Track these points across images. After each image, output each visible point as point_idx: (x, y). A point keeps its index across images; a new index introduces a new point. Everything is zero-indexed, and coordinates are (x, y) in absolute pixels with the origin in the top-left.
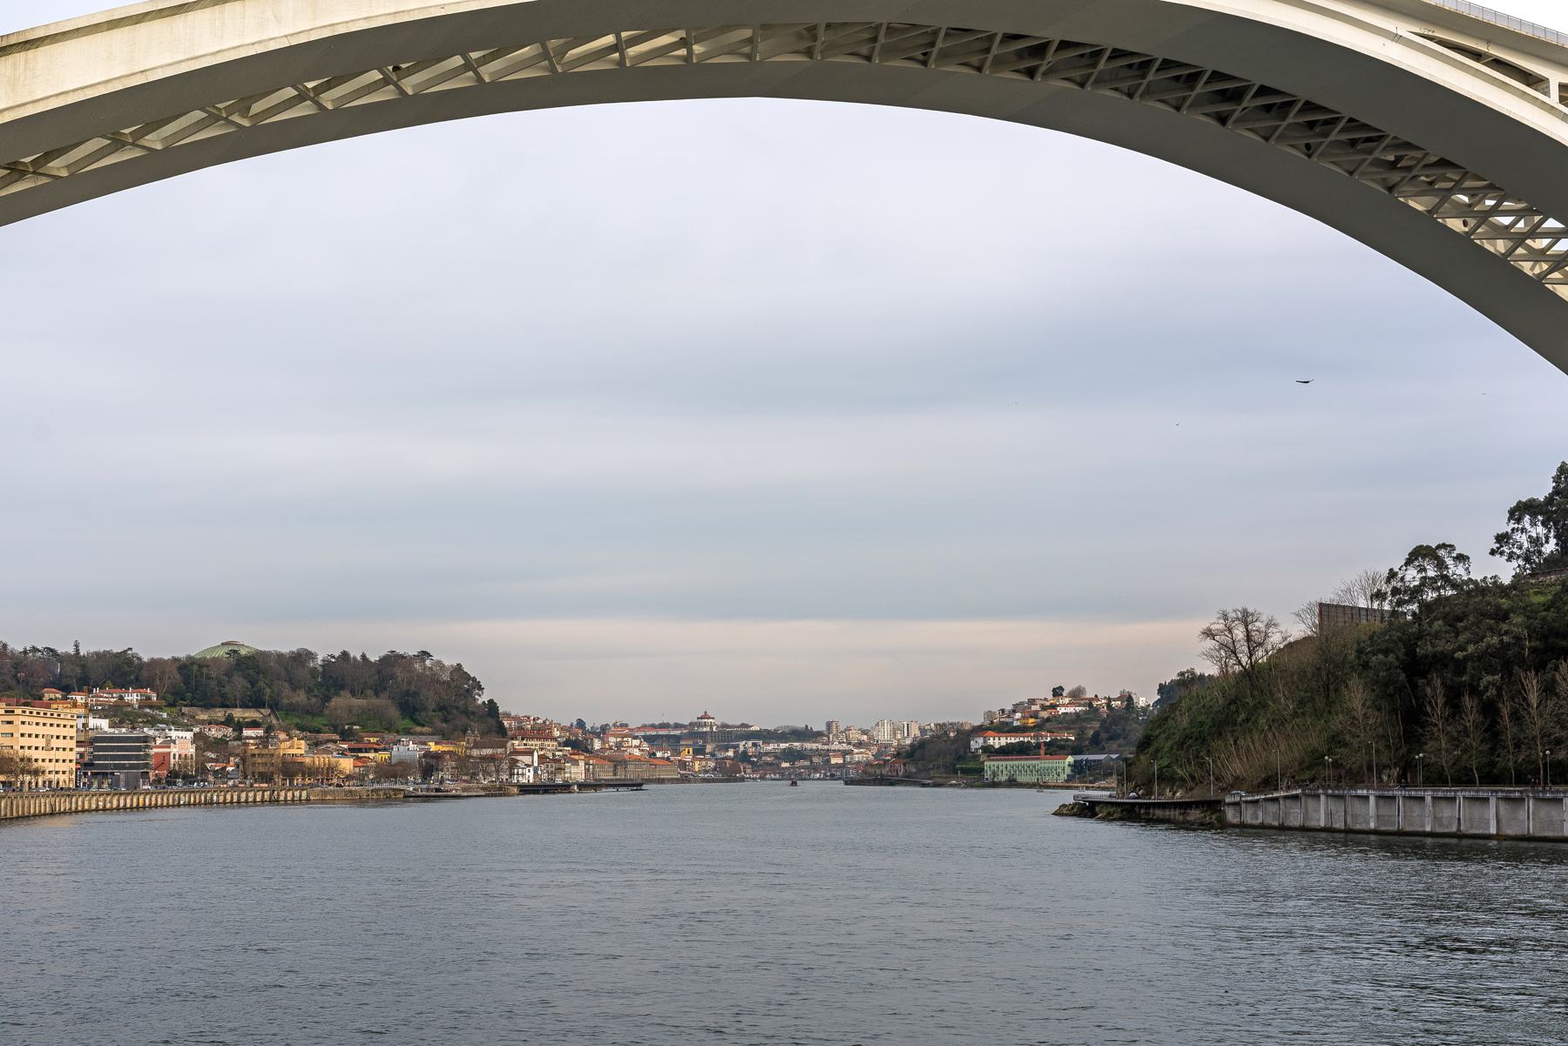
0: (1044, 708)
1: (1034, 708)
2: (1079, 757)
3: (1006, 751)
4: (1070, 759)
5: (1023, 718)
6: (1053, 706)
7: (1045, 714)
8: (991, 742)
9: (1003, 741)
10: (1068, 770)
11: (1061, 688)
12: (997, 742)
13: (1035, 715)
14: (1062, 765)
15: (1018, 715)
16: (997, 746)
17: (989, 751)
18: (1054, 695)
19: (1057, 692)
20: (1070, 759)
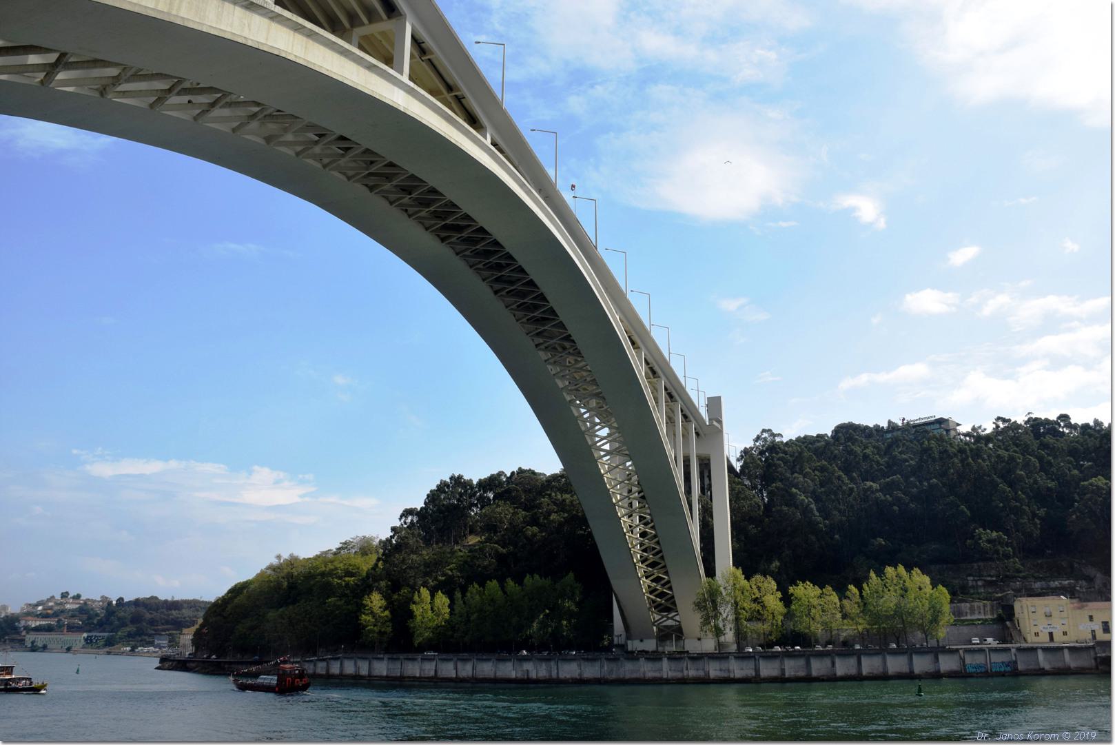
0: (57, 604)
1: (50, 604)
2: (90, 634)
3: (38, 629)
4: (85, 635)
5: (44, 609)
6: (61, 604)
7: (56, 608)
8: (30, 623)
9: (38, 623)
10: (83, 642)
11: (67, 593)
12: (34, 623)
13: (51, 608)
14: (79, 638)
15: (40, 608)
16: (33, 626)
17: (28, 629)
18: (62, 597)
19: (65, 595)
20: (85, 635)
